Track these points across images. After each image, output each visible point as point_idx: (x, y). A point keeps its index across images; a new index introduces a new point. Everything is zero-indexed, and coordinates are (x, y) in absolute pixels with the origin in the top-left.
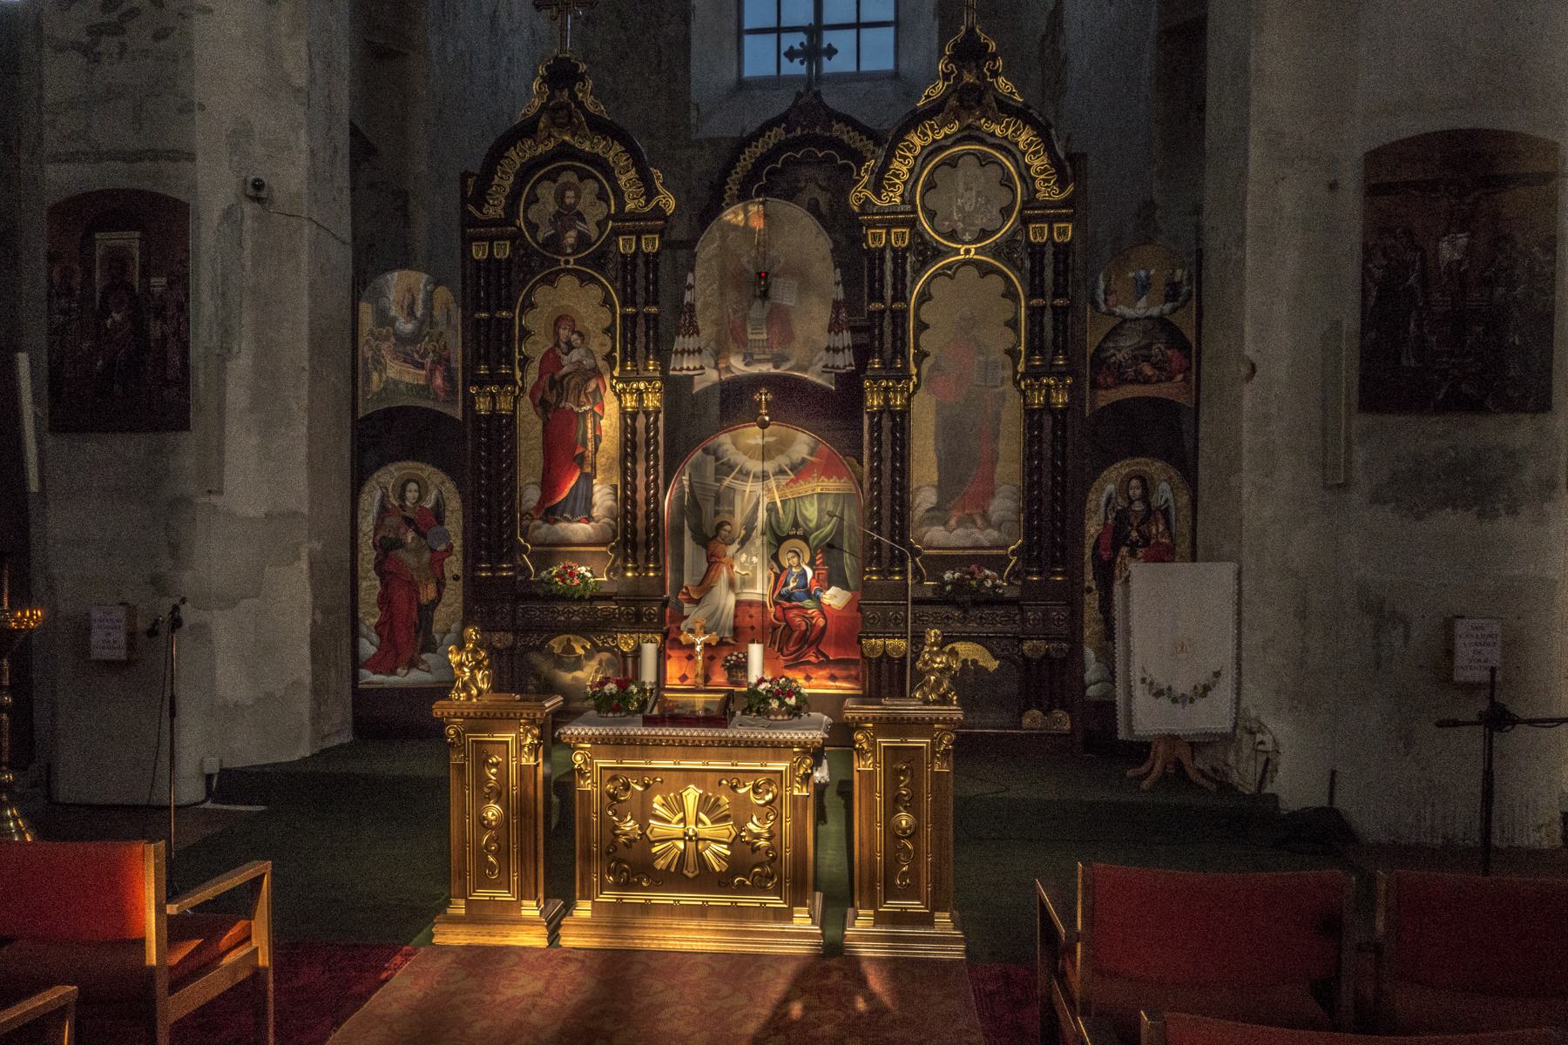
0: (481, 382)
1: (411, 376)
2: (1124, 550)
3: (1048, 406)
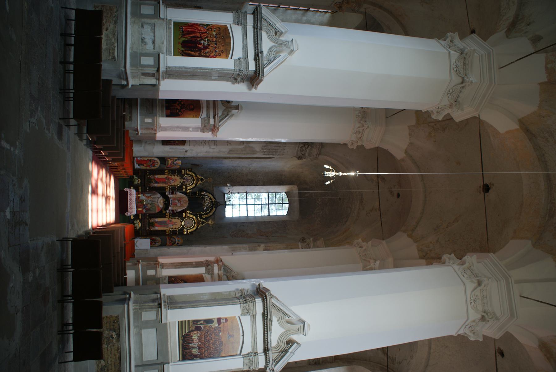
0: (169, 171)
1: (169, 163)
3: (166, 232)
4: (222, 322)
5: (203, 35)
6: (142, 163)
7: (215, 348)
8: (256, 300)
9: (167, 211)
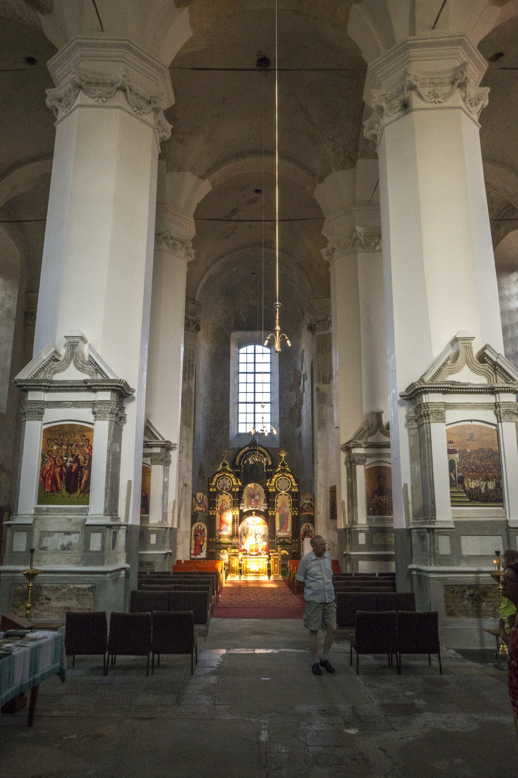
0: (211, 510)
1: (200, 509)
4: (453, 448)
5: (57, 463)
7: (487, 458)
8: (424, 401)
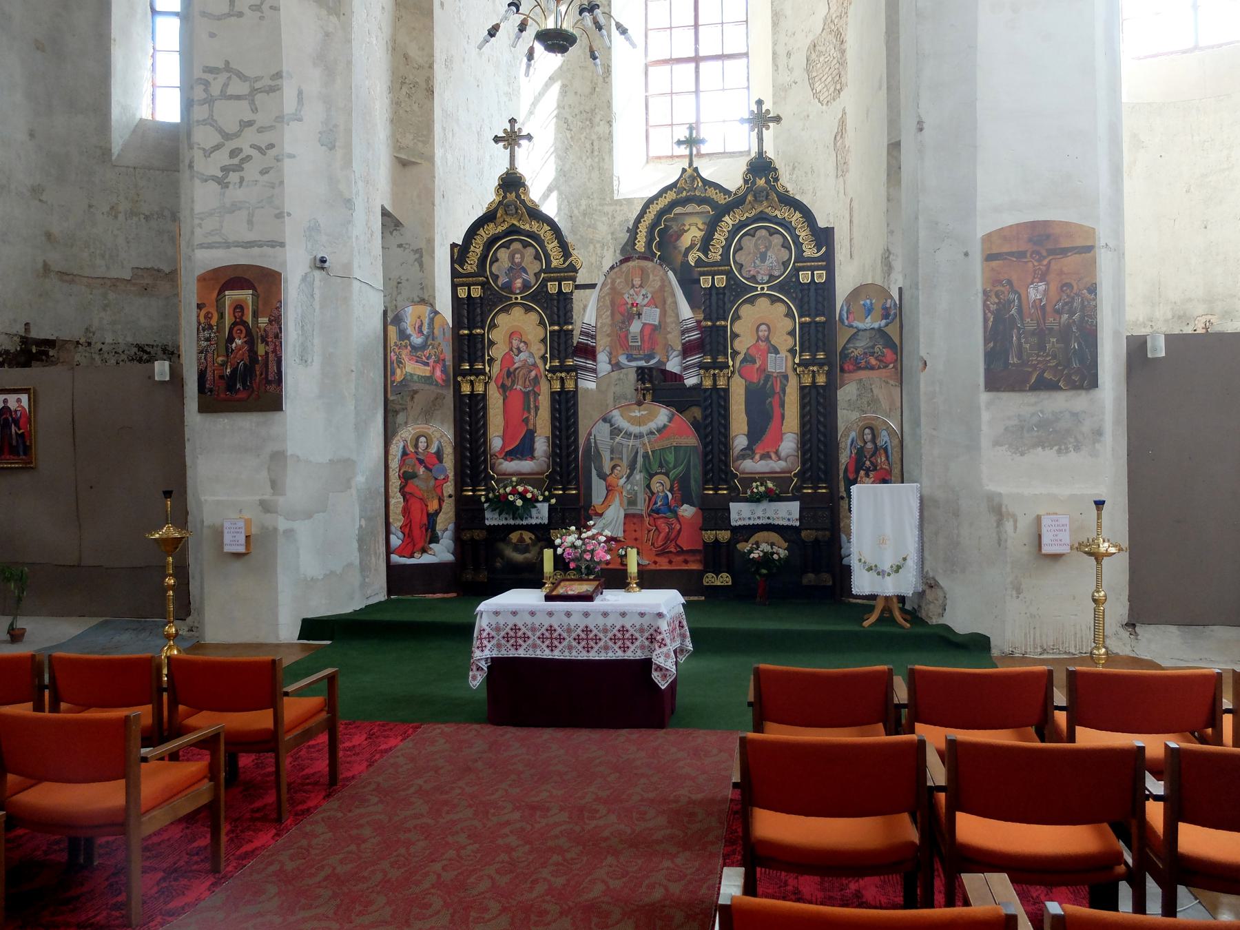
0: (464, 374)
2: (862, 473)
6: (425, 520)
9: (691, 381)
